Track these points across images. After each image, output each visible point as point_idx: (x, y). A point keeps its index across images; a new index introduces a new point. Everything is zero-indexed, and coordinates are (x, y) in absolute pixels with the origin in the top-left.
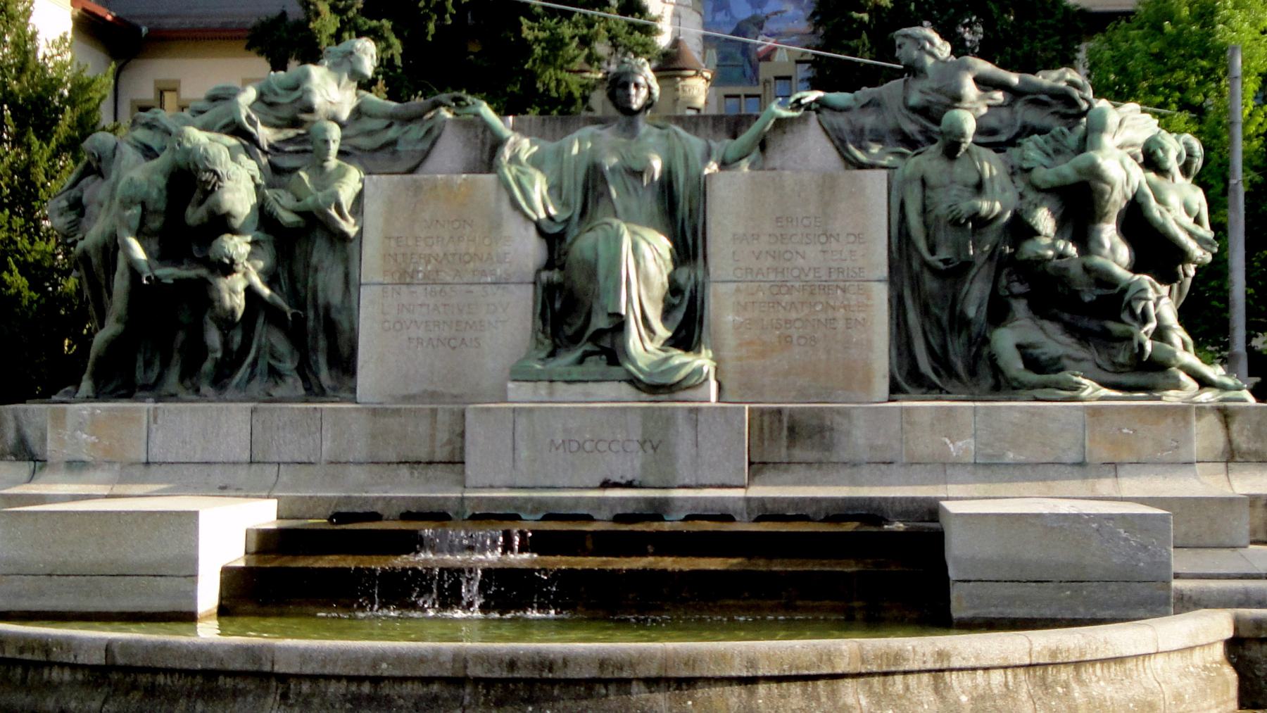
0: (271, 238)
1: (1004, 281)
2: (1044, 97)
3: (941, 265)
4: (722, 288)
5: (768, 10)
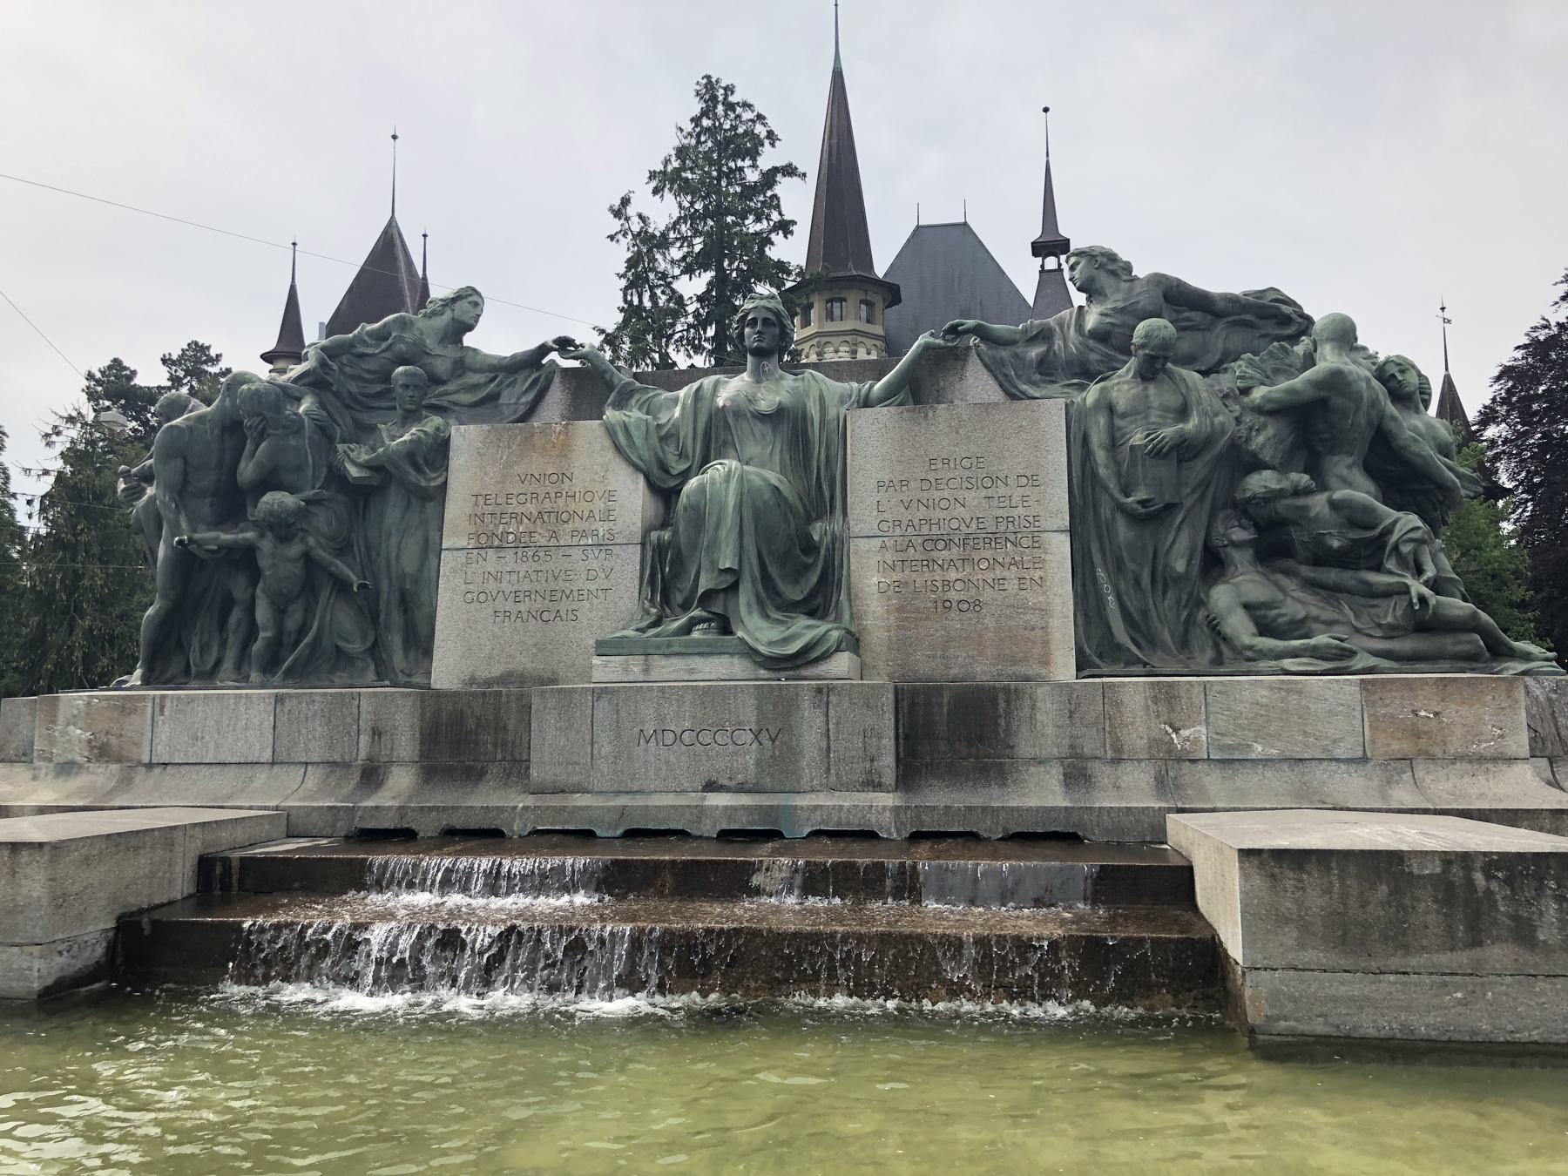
2: (1248, 317)
3: (1141, 510)
4: (863, 545)
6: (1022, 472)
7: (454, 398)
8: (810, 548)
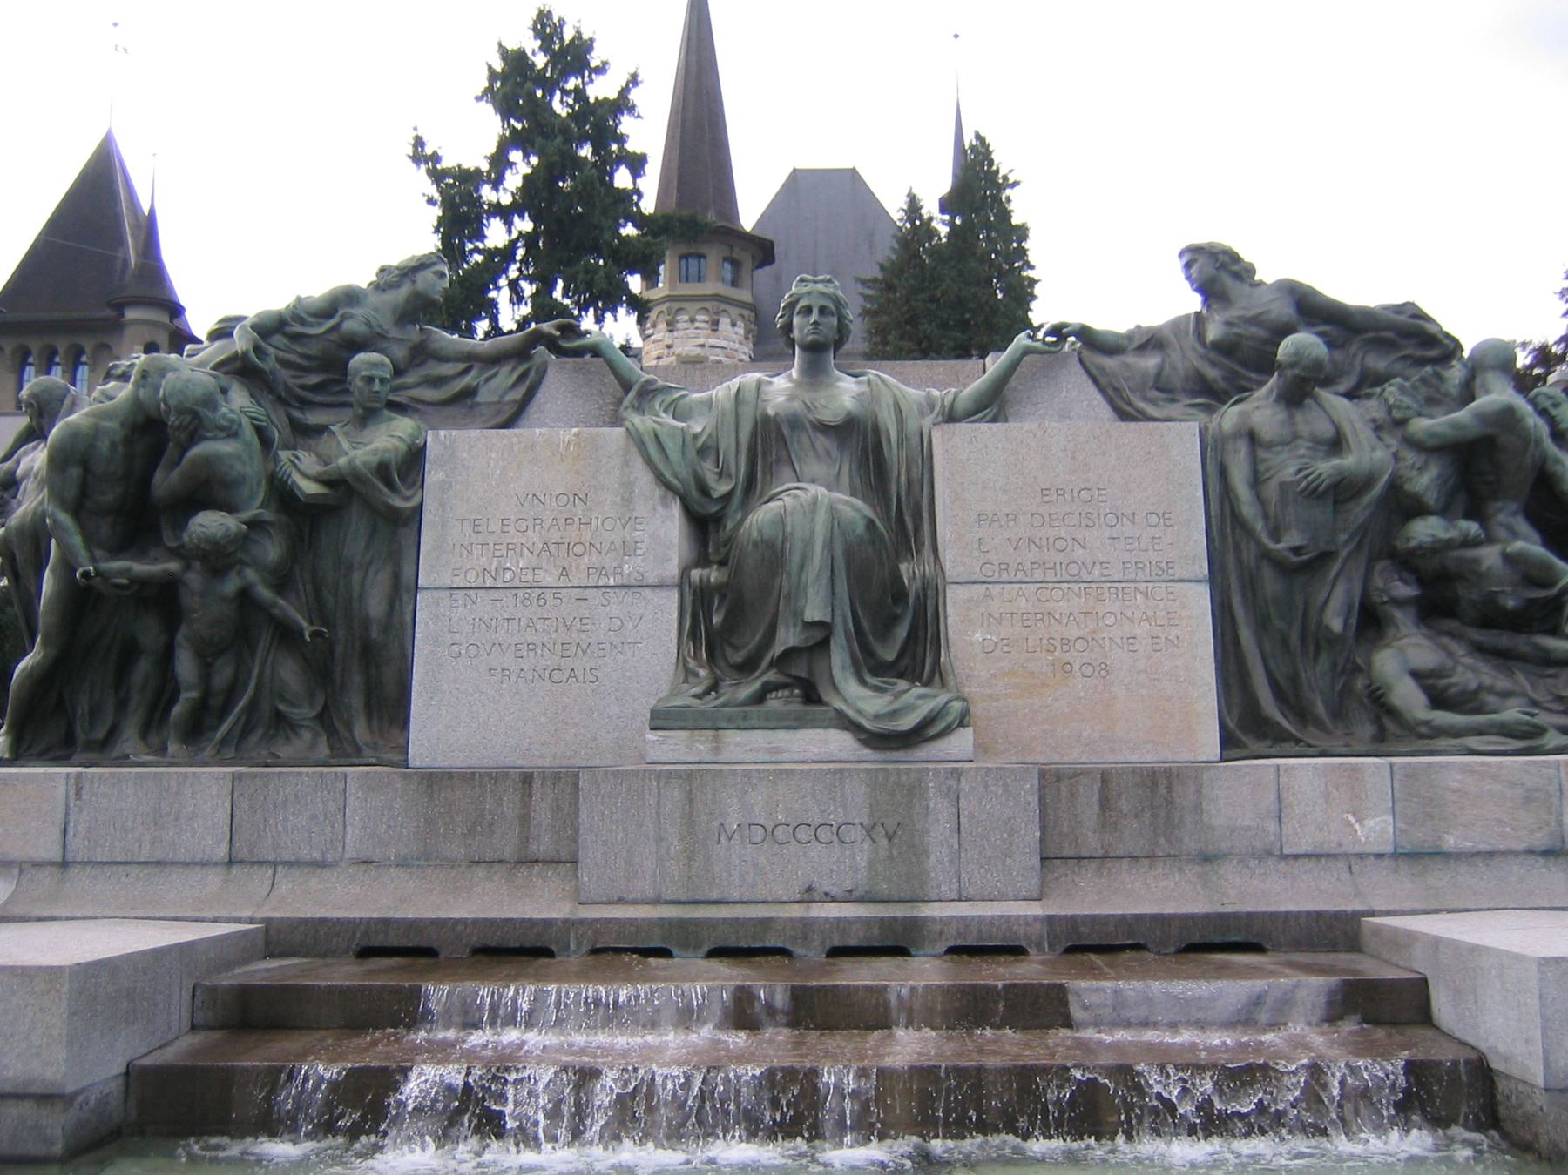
0: (284, 518)
1: (1378, 582)
2: (1389, 335)
3: (1295, 559)
6: (1151, 509)
7: (415, 393)
8: (900, 595)
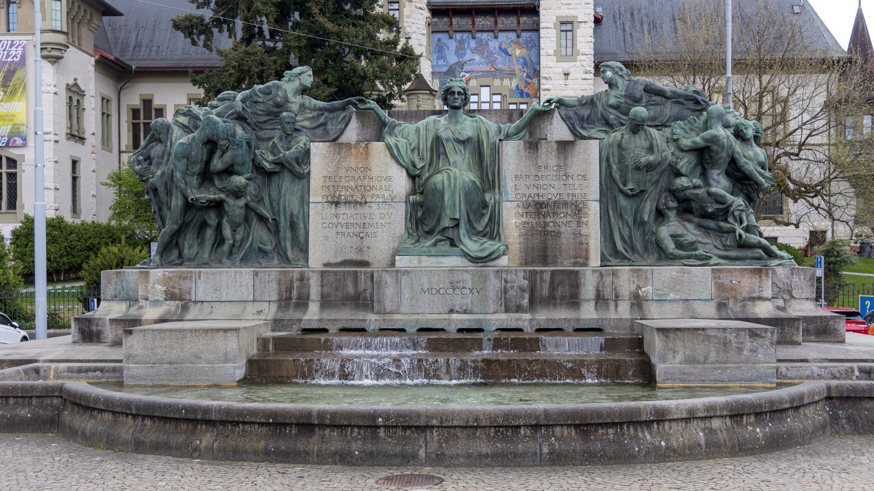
2: (681, 100)
5: (466, 58)
8: (485, 206)
